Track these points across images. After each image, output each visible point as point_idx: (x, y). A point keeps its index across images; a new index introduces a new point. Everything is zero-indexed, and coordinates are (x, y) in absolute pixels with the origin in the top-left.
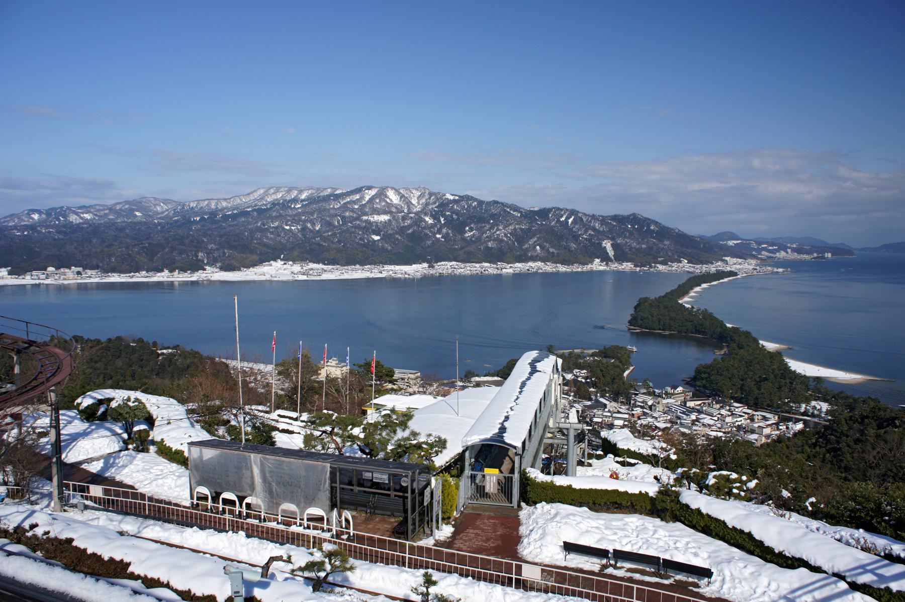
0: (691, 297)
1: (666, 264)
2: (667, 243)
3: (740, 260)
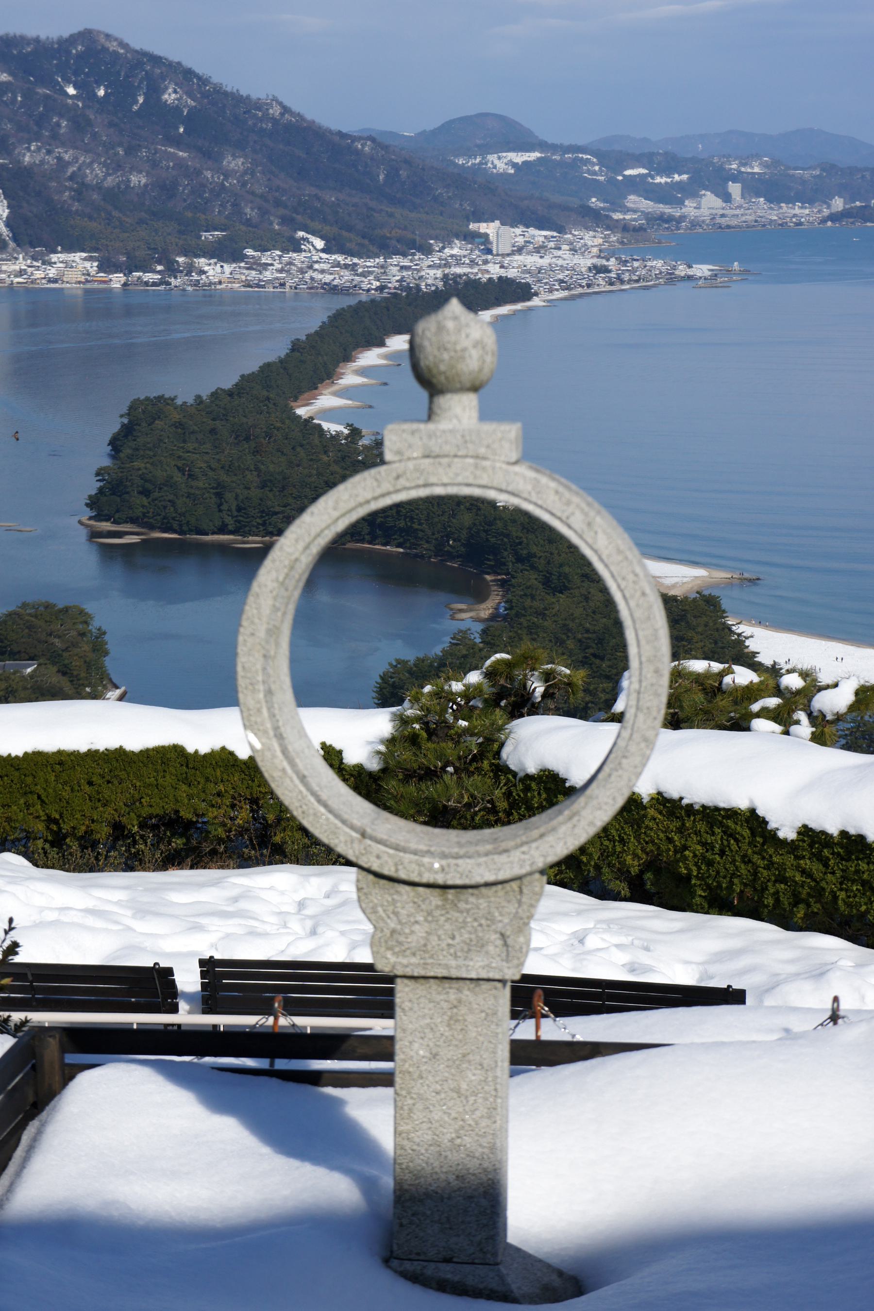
0: (342, 393)
1: (236, 256)
2: (235, 163)
3: (539, 235)
